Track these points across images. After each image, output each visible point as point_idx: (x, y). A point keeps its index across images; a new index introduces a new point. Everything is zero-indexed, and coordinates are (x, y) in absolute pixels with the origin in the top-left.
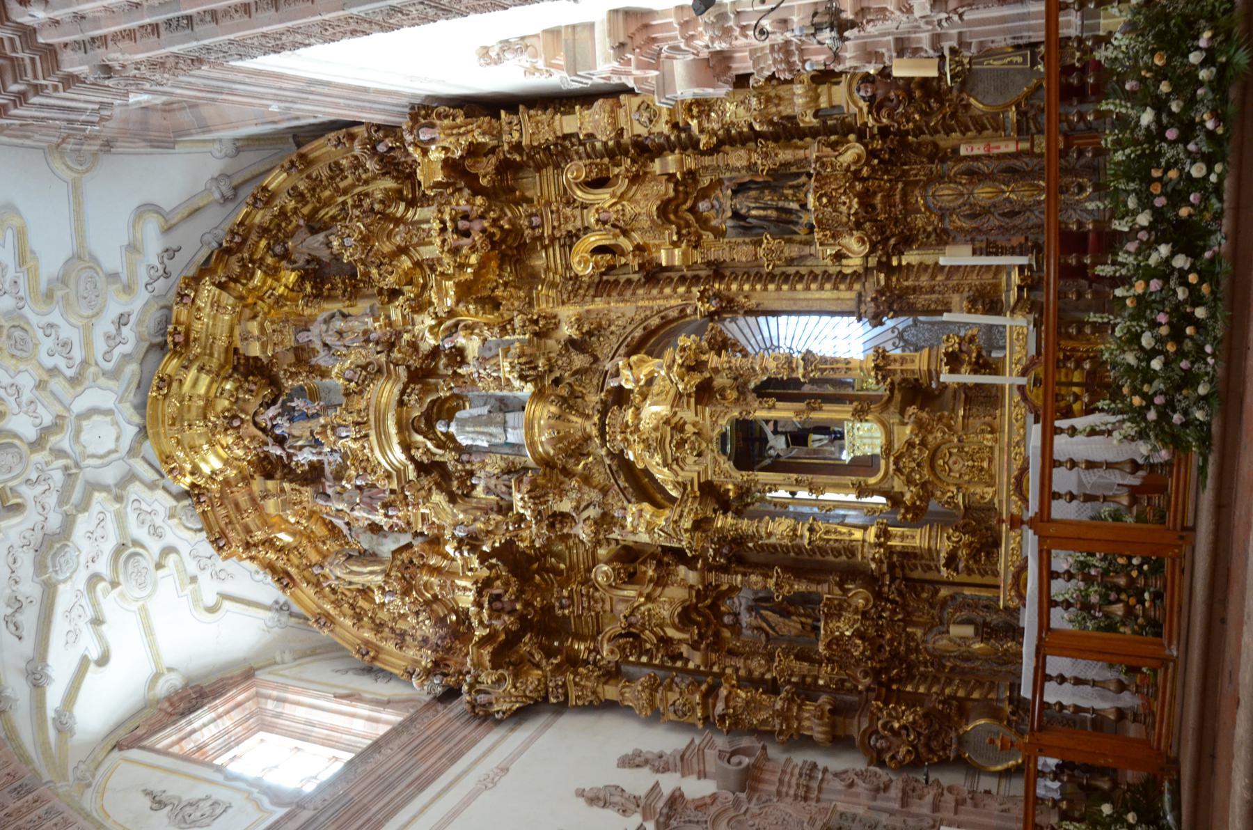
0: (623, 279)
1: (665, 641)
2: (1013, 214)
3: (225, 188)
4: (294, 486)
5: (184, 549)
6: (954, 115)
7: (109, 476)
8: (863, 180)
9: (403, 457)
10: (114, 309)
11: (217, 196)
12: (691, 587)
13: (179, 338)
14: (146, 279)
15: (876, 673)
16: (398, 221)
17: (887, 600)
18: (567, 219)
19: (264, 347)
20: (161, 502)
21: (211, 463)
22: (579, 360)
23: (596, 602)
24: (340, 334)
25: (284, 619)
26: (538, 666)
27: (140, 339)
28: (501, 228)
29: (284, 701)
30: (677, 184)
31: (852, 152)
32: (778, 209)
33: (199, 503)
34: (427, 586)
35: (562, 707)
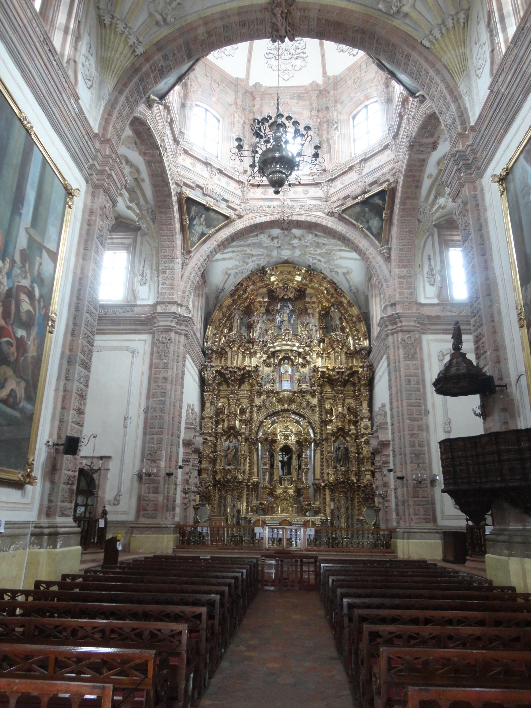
0: (323, 413)
1: (223, 421)
2: (338, 517)
3: (355, 291)
9: (278, 348)
10: (323, 260)
19: (308, 302)
20: (262, 262)
21: (273, 279)
22: (304, 405)
24: (312, 330)
26: (214, 382)
27: (313, 264)
33: (261, 273)
34: (234, 346)
35: (202, 390)
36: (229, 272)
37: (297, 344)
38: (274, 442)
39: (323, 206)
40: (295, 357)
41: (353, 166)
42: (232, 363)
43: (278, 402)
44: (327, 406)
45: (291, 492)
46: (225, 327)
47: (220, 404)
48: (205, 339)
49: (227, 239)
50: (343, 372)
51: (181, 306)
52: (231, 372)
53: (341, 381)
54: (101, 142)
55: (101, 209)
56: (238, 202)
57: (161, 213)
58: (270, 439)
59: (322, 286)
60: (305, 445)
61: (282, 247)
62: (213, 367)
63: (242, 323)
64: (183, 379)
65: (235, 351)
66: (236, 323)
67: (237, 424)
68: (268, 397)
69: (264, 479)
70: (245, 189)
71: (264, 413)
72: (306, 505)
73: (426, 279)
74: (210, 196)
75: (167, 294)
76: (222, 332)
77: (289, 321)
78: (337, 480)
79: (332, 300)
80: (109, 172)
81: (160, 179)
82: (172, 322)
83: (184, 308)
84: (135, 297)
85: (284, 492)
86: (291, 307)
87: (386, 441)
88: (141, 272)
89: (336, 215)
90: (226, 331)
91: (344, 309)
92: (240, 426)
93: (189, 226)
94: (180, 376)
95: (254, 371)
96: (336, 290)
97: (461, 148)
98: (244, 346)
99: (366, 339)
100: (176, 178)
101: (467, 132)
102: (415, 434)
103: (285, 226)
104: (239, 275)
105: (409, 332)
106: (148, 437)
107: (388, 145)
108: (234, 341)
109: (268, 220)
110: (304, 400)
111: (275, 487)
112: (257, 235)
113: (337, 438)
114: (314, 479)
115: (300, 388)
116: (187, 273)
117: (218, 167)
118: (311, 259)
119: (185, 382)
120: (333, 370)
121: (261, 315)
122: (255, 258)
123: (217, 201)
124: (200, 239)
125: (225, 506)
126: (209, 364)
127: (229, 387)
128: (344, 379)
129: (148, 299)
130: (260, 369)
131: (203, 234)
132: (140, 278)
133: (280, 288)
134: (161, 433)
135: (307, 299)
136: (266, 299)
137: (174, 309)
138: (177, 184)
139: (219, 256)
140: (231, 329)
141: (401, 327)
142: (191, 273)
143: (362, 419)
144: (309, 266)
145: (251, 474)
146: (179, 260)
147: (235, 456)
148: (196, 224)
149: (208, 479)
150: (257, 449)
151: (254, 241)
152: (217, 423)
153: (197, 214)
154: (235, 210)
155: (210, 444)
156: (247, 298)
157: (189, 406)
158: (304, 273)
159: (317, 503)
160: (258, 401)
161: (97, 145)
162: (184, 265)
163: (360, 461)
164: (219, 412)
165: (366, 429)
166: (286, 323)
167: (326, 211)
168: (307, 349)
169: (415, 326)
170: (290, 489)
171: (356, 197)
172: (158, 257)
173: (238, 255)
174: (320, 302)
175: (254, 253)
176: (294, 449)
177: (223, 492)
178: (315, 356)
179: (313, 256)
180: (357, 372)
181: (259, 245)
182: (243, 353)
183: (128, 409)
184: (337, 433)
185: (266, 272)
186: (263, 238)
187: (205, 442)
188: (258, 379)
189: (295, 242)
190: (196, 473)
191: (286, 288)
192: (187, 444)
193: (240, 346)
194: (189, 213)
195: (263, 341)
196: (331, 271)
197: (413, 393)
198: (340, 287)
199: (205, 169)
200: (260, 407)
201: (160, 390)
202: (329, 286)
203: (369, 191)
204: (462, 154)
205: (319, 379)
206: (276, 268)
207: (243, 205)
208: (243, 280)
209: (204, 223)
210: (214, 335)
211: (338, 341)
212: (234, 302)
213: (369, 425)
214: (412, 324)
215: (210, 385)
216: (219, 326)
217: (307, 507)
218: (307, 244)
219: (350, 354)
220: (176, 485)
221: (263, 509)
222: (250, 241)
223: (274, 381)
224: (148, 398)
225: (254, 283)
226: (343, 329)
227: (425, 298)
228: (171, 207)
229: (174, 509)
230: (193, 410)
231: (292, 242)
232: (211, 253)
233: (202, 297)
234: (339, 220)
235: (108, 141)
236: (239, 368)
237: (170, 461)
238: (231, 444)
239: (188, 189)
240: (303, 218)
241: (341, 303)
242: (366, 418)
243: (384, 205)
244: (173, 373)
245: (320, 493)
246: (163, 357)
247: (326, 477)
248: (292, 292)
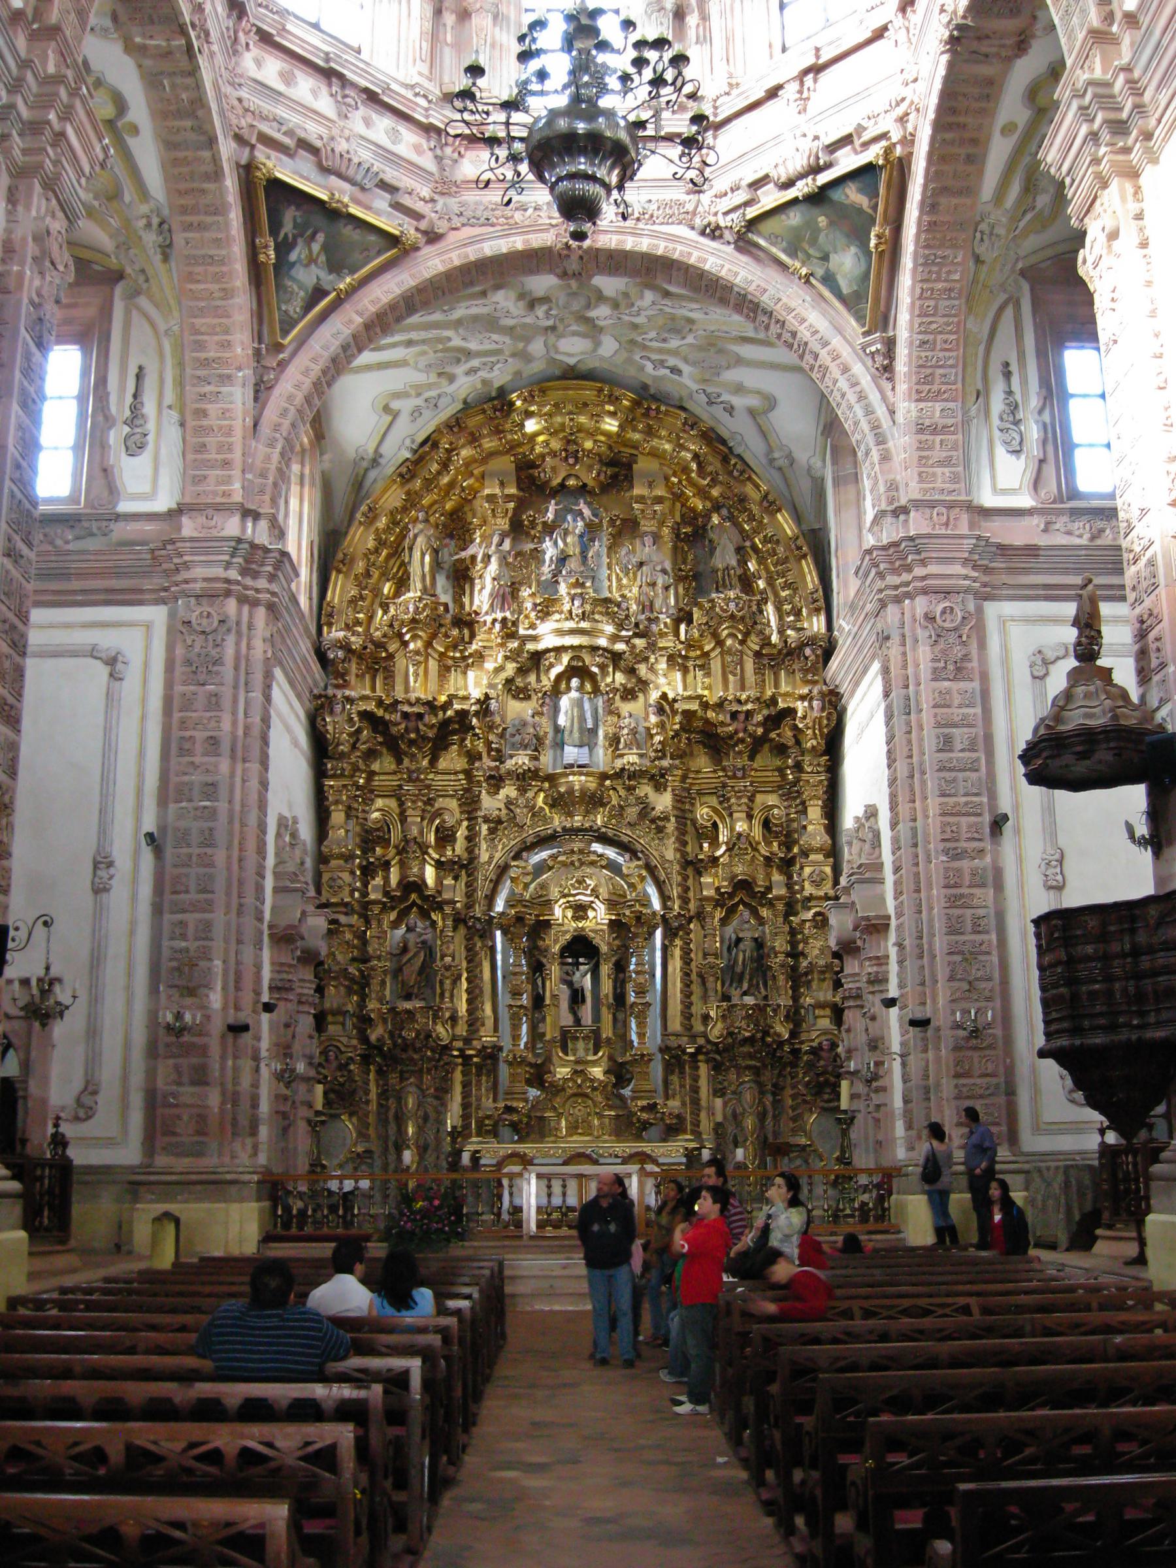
0: (688, 838)
1: (386, 865)
4: (510, 514)
5: (450, 389)
6: (805, 1102)
7: (537, 347)
8: (763, 1039)
10: (686, 369)
11: (776, 455)
12: (439, 892)
13: (653, 414)
14: (709, 390)
15: (379, 1048)
16: (743, 642)
17: (441, 1055)
18: (739, 798)
19: (641, 499)
20: (499, 376)
21: (531, 426)
22: (632, 812)
23: (414, 802)
24: (654, 584)
25: (365, 464)
26: (354, 747)
27: (655, 378)
28: (736, 745)
29: (302, 484)
30: (764, 894)
31: (782, 1030)
32: (743, 973)
33: (495, 410)
35: (319, 773)
36: (395, 405)
37: (609, 629)
38: (543, 926)
39: (690, 207)
40: (602, 667)
41: (780, 87)
42: (407, 690)
43: (552, 806)
44: (702, 813)
45: (597, 1072)
46: (384, 576)
47: (376, 815)
48: (323, 614)
49: (393, 306)
50: (749, 714)
51: (256, 516)
52: (406, 715)
53: (742, 741)
54: (33, 37)
55: (37, 239)
56: (425, 192)
57: (189, 227)
58: (530, 919)
59: (682, 447)
60: (636, 935)
61: (561, 328)
62: (349, 700)
63: (437, 565)
64: (265, 741)
65: (417, 653)
66: (420, 562)
67: (430, 874)
68: (522, 790)
69: (516, 1037)
70: (448, 150)
71: (508, 842)
72: (643, 1109)
73: (997, 433)
74: (340, 175)
75: (211, 481)
76: (377, 592)
77: (584, 558)
78: (731, 1034)
79: (715, 492)
80: (57, 126)
81: (188, 123)
82: (228, 565)
83: (263, 524)
84: (113, 490)
85: (576, 1072)
86: (587, 512)
87: (878, 917)
88: (128, 413)
89: (728, 236)
90: (387, 588)
91: (752, 518)
92: (439, 880)
93: (276, 267)
94: (256, 732)
95: (477, 714)
96: (725, 460)
97: (1098, 74)
98: (447, 636)
99: (817, 610)
100: (234, 121)
101: (1115, 29)
102: (962, 896)
103: (573, 265)
104: (427, 414)
105: (947, 593)
106: (167, 917)
107: (885, 28)
108: (414, 621)
109: (520, 246)
110: (632, 799)
111: (548, 1059)
112: (484, 294)
113: (732, 911)
114: (665, 1033)
115: (619, 764)
116: (270, 414)
117: (364, 83)
118: (649, 367)
119: (272, 751)
120: (720, 705)
121: (496, 539)
122: (475, 363)
123: (363, 189)
124: (308, 307)
125: (400, 1120)
126: (339, 694)
127: (399, 762)
128: (750, 735)
129: (151, 496)
130: (493, 705)
131: (319, 293)
132: (127, 429)
133: (554, 454)
134: (208, 906)
135: (637, 491)
136: (512, 490)
137: (232, 526)
138: (239, 139)
139: (366, 357)
140: (402, 584)
141: (924, 578)
142: (284, 413)
143: (805, 854)
144: (645, 387)
145: (474, 1022)
146: (246, 374)
147: (426, 970)
148: (299, 260)
149: (344, 1040)
150: (493, 949)
151: (474, 311)
152: (368, 872)
153: (301, 229)
154: (417, 216)
155: (348, 936)
156: (452, 485)
157: (282, 823)
158: (631, 410)
159: (674, 1104)
160: (490, 804)
161: (21, 43)
162: (261, 390)
163: (798, 979)
164: (371, 838)
165: (817, 884)
166: (573, 564)
167: (698, 222)
168: (640, 643)
169: (966, 577)
170: (594, 1063)
171: (789, 184)
172: (180, 365)
173: (424, 353)
174: (678, 497)
175: (473, 346)
176: (604, 948)
177: (393, 1079)
178: (662, 665)
179: (654, 357)
180: (791, 712)
181: (490, 323)
182: (442, 655)
183: (103, 830)
184: (731, 895)
185: (512, 404)
186: (504, 301)
187: (334, 930)
188: (492, 737)
189: (601, 312)
190: (306, 1023)
191: (571, 452)
192: (284, 937)
193: (434, 636)
194: (275, 227)
195: (504, 620)
196: (710, 403)
197: (961, 775)
198: (739, 450)
199: (324, 90)
200: (499, 821)
201: (196, 778)
202: (705, 449)
203: (829, 166)
204: (1100, 91)
205: (677, 734)
206: (543, 391)
207: (441, 201)
208: (437, 430)
209: (322, 258)
210: (353, 601)
211: (732, 617)
212: (412, 501)
213: (828, 870)
214: (958, 569)
215: (342, 756)
216: (368, 575)
217: (645, 1116)
218: (639, 320)
219: (771, 657)
220: (256, 1058)
221: (514, 1127)
222: (459, 313)
223: (538, 744)
224: (163, 800)
225: (474, 439)
226: (747, 583)
227: (995, 490)
228: (219, 210)
229: (254, 1131)
230: (294, 835)
231: (592, 314)
232: (345, 348)
233: (312, 484)
234: (739, 249)
235: (54, 31)
236: (431, 705)
237: (238, 988)
238: (411, 936)
239: (274, 154)
240: (629, 244)
241: (743, 499)
242: (819, 850)
243: (875, 208)
244: (234, 723)
245: (682, 1072)
246: (202, 678)
247: (698, 1027)
248: (590, 468)
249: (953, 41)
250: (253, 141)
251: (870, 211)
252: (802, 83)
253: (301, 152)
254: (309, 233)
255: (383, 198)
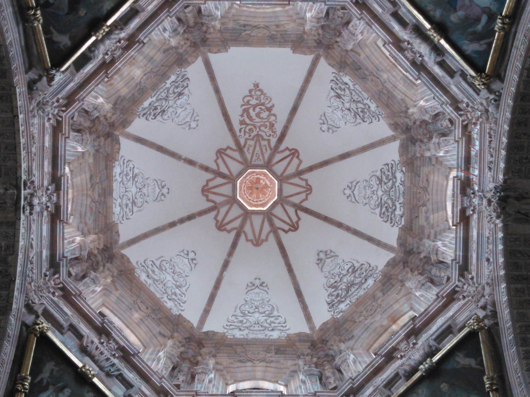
41: (395, 349)
117: (122, 343)
171: (415, 370)
203: (438, 350)
243: (481, 363)
249: (503, 202)
250: (40, 312)
251: (478, 367)
252: (408, 343)
253: (70, 333)
254: (59, 385)
255: (120, 388)
